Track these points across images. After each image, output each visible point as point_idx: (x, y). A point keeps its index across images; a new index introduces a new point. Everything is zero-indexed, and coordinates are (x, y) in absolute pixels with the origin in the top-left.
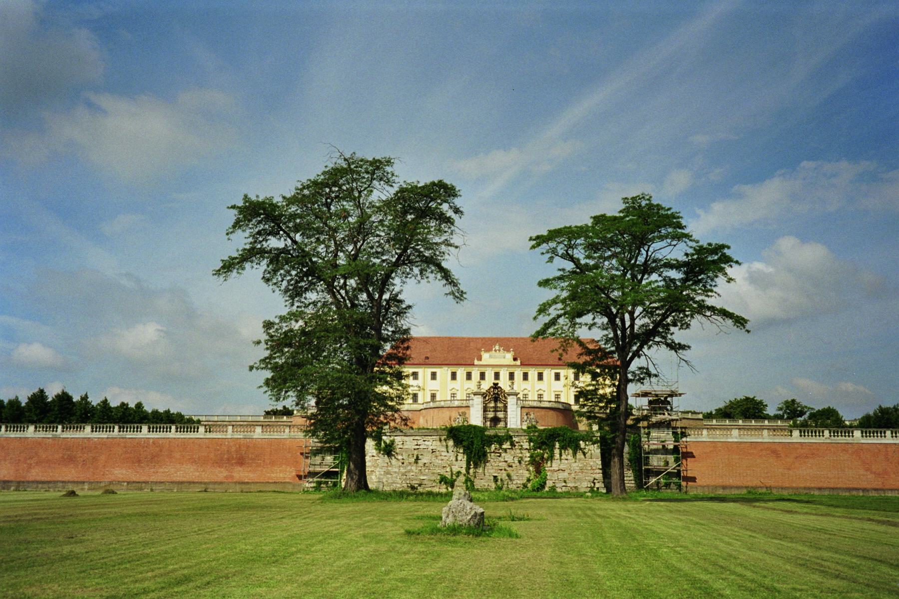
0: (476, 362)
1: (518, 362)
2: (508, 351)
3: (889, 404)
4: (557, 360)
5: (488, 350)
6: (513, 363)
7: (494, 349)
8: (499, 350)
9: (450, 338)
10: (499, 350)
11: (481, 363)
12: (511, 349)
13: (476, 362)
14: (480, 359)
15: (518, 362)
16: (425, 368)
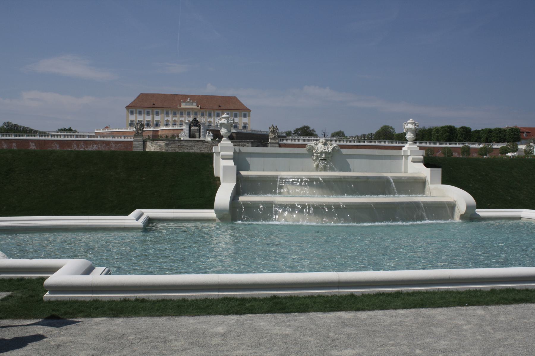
2: (195, 102)
5: (184, 102)
9: (164, 94)
10: (190, 101)
13: (178, 107)
14: (180, 105)
15: (199, 108)
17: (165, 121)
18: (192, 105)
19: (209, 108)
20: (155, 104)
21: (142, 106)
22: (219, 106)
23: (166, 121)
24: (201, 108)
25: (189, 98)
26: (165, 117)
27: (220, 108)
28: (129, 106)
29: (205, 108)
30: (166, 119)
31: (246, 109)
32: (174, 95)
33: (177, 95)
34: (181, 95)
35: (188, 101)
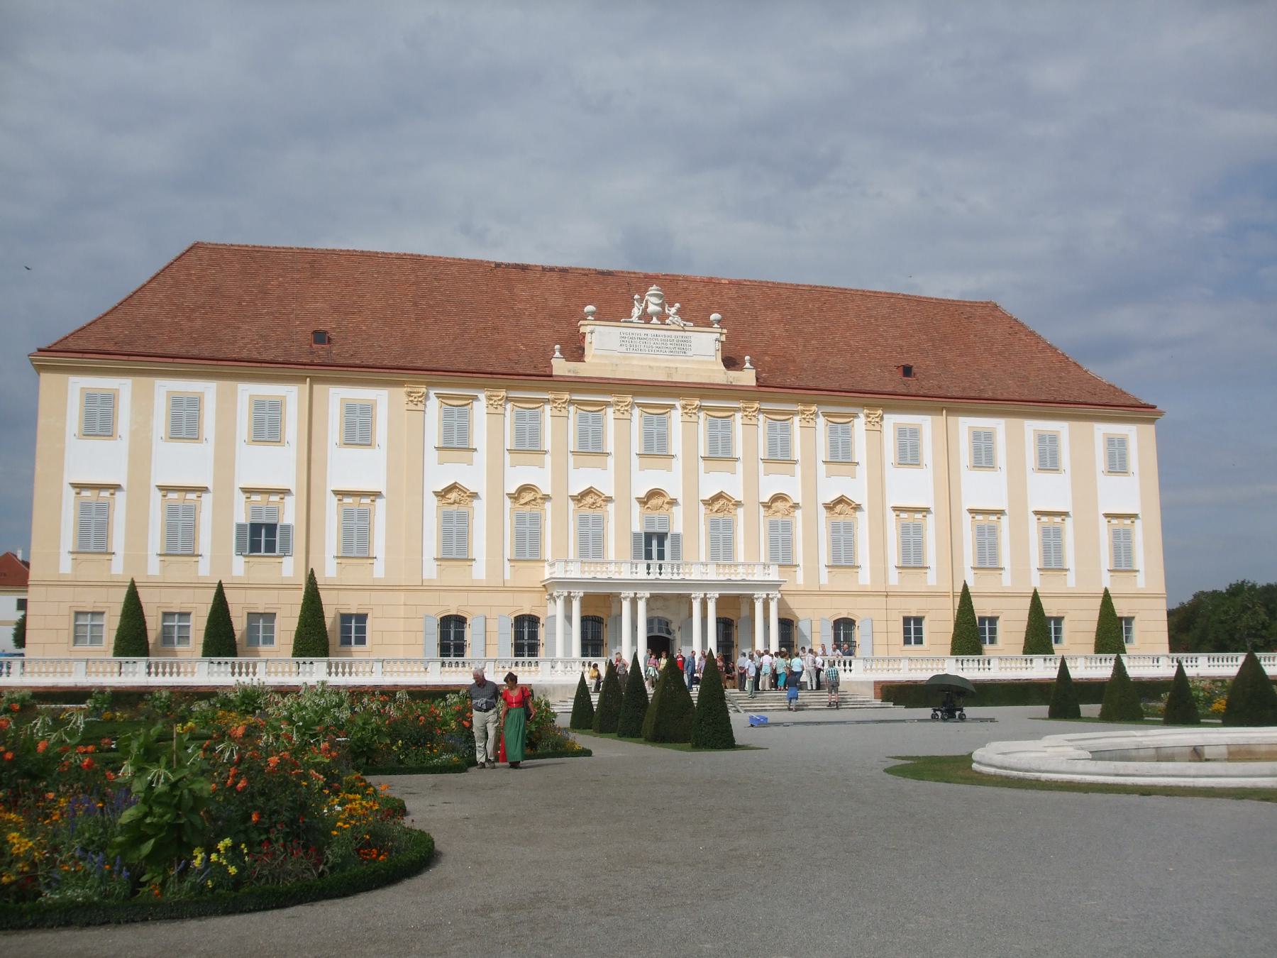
0: (560, 366)
1: (747, 377)
2: (703, 322)
3: (1272, 582)
4: (899, 375)
5: (614, 311)
6: (720, 375)
7: (636, 312)
8: (662, 317)
10: (662, 317)
11: (584, 369)
12: (715, 316)
13: (560, 366)
14: (576, 351)
15: (747, 377)
16: (315, 380)
17: (431, 503)
18: (683, 347)
19: (822, 386)
20: (333, 335)
21: (206, 349)
22: (907, 371)
23: (442, 495)
24: (760, 382)
25: (654, 289)
26: (432, 456)
27: (913, 385)
28: (72, 345)
29: (790, 381)
30: (439, 474)
31: (1122, 401)
32: (498, 265)
33: (524, 268)
34: (564, 271)
35: (646, 317)
